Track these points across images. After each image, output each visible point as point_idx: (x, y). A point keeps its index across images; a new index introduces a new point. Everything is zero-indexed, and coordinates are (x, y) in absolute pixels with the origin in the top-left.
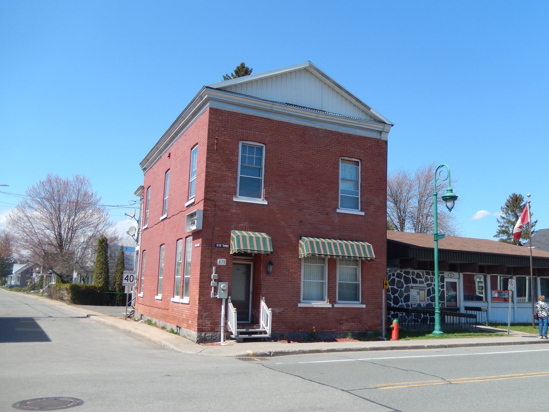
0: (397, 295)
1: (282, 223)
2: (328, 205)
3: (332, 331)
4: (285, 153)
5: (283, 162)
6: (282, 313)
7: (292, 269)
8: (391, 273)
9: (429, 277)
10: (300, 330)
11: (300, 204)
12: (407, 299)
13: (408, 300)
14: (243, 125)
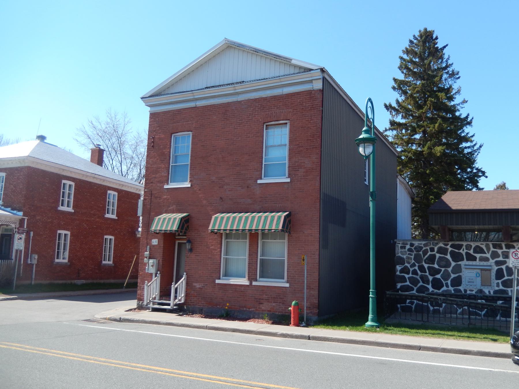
0: (438, 276)
1: (204, 202)
2: (249, 178)
3: (250, 310)
4: (208, 135)
5: (206, 143)
6: (202, 289)
7: (212, 245)
8: (428, 248)
9: (500, 251)
10: (218, 306)
11: (221, 181)
12: (457, 282)
13: (460, 284)
14: (174, 119)
